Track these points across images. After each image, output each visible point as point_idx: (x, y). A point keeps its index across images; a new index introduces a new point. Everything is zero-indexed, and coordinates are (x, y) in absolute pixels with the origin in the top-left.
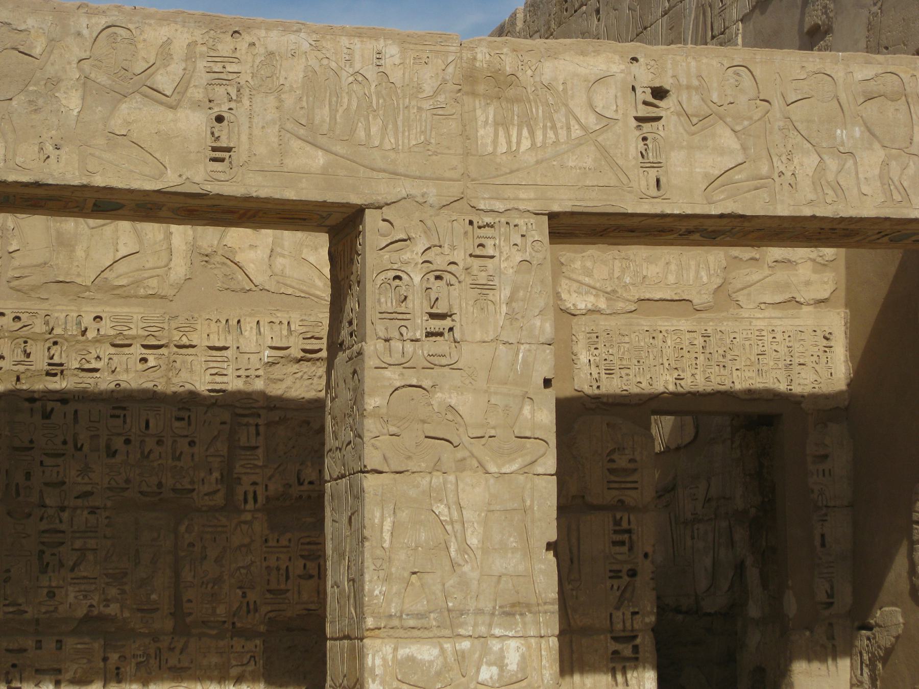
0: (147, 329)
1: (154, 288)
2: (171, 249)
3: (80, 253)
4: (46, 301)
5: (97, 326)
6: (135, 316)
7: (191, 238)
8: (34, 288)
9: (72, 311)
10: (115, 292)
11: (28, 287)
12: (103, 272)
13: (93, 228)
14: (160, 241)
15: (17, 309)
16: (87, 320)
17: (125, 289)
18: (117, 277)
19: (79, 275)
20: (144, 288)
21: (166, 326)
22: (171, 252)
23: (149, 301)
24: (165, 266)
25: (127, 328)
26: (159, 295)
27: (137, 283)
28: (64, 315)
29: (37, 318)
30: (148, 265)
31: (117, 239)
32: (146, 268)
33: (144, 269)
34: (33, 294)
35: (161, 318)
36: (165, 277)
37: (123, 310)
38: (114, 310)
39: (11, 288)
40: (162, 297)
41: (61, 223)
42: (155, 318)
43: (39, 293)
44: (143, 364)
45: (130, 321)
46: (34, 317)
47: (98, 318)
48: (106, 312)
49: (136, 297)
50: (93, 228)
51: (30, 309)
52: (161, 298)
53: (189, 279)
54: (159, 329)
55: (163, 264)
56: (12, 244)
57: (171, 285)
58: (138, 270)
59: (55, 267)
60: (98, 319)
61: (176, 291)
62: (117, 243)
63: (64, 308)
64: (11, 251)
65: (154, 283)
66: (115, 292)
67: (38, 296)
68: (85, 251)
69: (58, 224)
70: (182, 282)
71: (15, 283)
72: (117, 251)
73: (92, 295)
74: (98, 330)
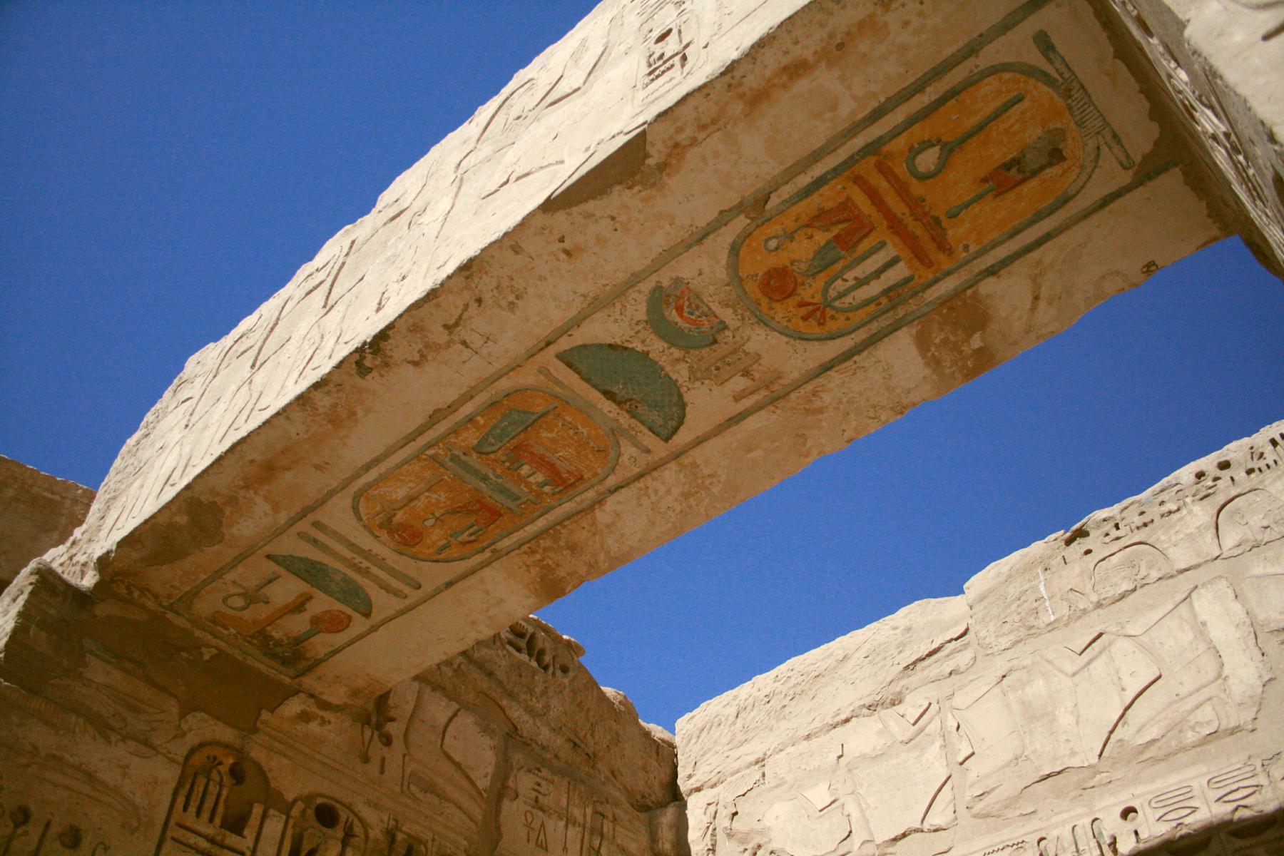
0: (1226, 799)
1: (1208, 723)
2: (1215, 648)
3: (1065, 719)
4: (1032, 816)
5: (1129, 826)
6: (1195, 784)
7: (1243, 615)
8: (1010, 803)
9: (1080, 816)
10: (1145, 756)
11: (998, 806)
12: (1111, 732)
13: (1074, 674)
14: (1191, 643)
15: (992, 846)
16: (1111, 824)
17: (1157, 745)
18: (1139, 731)
19: (1073, 753)
20: (1193, 728)
21: (1262, 779)
22: (1218, 652)
23: (1212, 748)
24: (1216, 679)
25: (1188, 811)
26: (1226, 730)
27: (1177, 726)
28: (1069, 827)
29: (1025, 850)
30: (1184, 691)
31: (1117, 672)
32: (1181, 696)
33: (1180, 698)
34: (1011, 813)
35: (1247, 769)
36: (1223, 695)
37: (1169, 781)
38: (1151, 787)
39: (974, 817)
40: (1233, 731)
41: (1023, 690)
42: (1235, 773)
43: (1019, 808)
44: (1134, 819)
45: (1189, 795)
46: (1021, 850)
47: (1127, 812)
48: (1138, 796)
49: (1184, 749)
50: (1074, 674)
51: (1008, 840)
52: (1232, 733)
53: (1270, 680)
54: (1251, 790)
55: (1211, 675)
56: (960, 750)
57: (1240, 704)
58: (1170, 704)
59: (1032, 757)
60: (1132, 815)
61: (1255, 709)
62: (1120, 678)
63: (1065, 816)
64: (961, 760)
65: (1206, 713)
66: (1145, 756)
67: (1017, 813)
68: (1072, 713)
69: (1020, 692)
70: (1260, 689)
71: (979, 807)
72: (1123, 689)
73: (1107, 777)
74: (1136, 833)
